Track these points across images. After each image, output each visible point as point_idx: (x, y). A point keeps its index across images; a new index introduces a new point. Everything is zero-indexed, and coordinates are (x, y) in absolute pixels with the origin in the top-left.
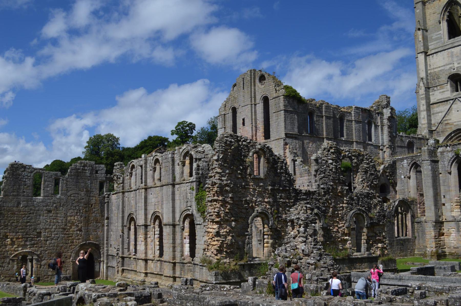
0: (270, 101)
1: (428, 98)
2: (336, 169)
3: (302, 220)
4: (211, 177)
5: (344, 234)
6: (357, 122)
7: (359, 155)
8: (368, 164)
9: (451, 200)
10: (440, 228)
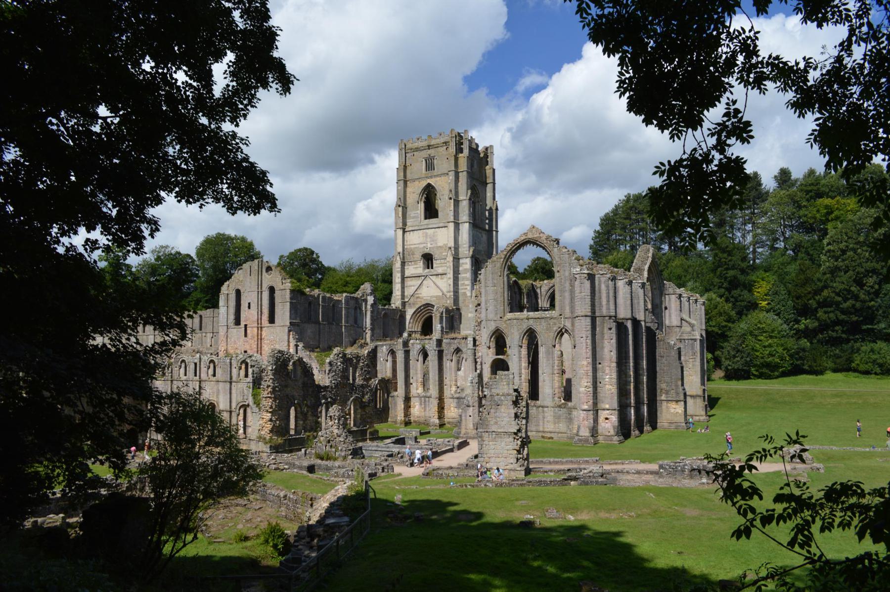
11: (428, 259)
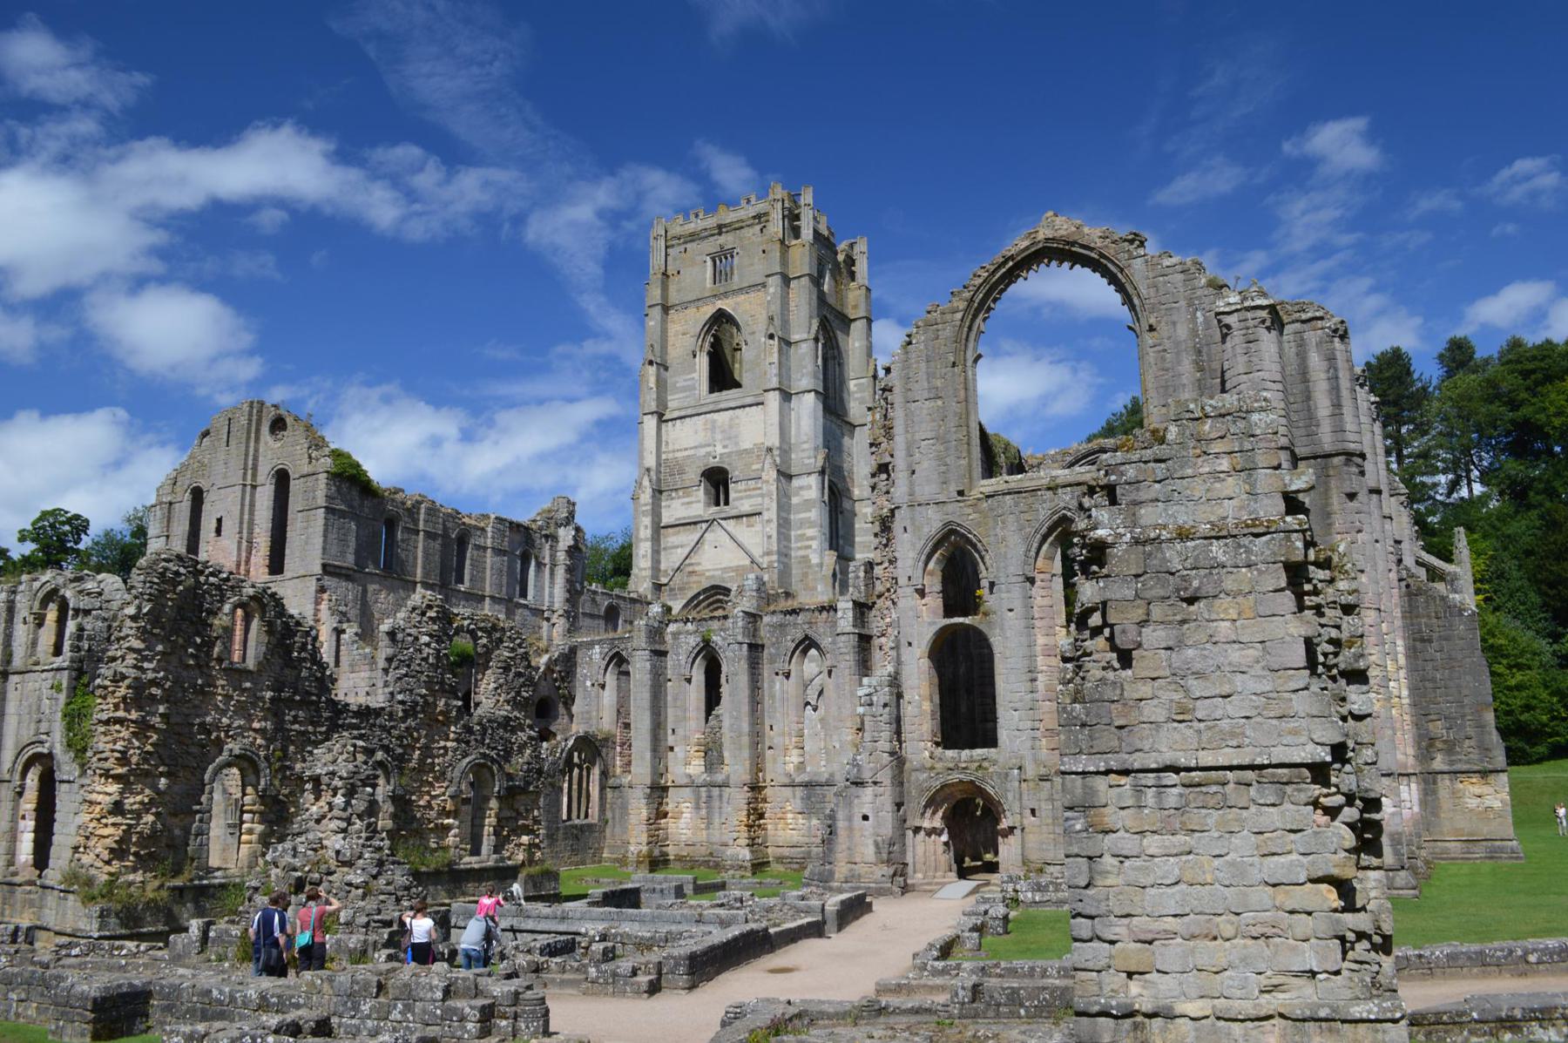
0: (292, 483)
1: (656, 513)
2: (438, 657)
3: (341, 778)
4: (114, 659)
5: (444, 813)
6: (498, 552)
7: (494, 628)
8: (513, 650)
9: (686, 738)
11: (717, 481)
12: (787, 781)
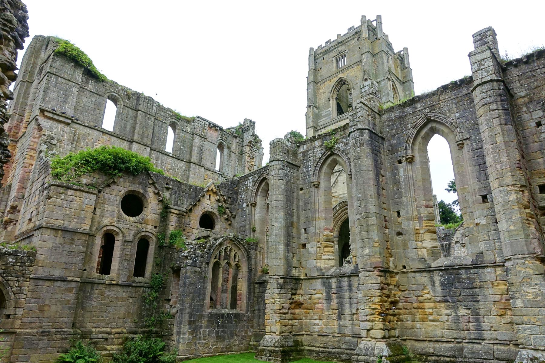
10: (294, 292)
12: (421, 266)
